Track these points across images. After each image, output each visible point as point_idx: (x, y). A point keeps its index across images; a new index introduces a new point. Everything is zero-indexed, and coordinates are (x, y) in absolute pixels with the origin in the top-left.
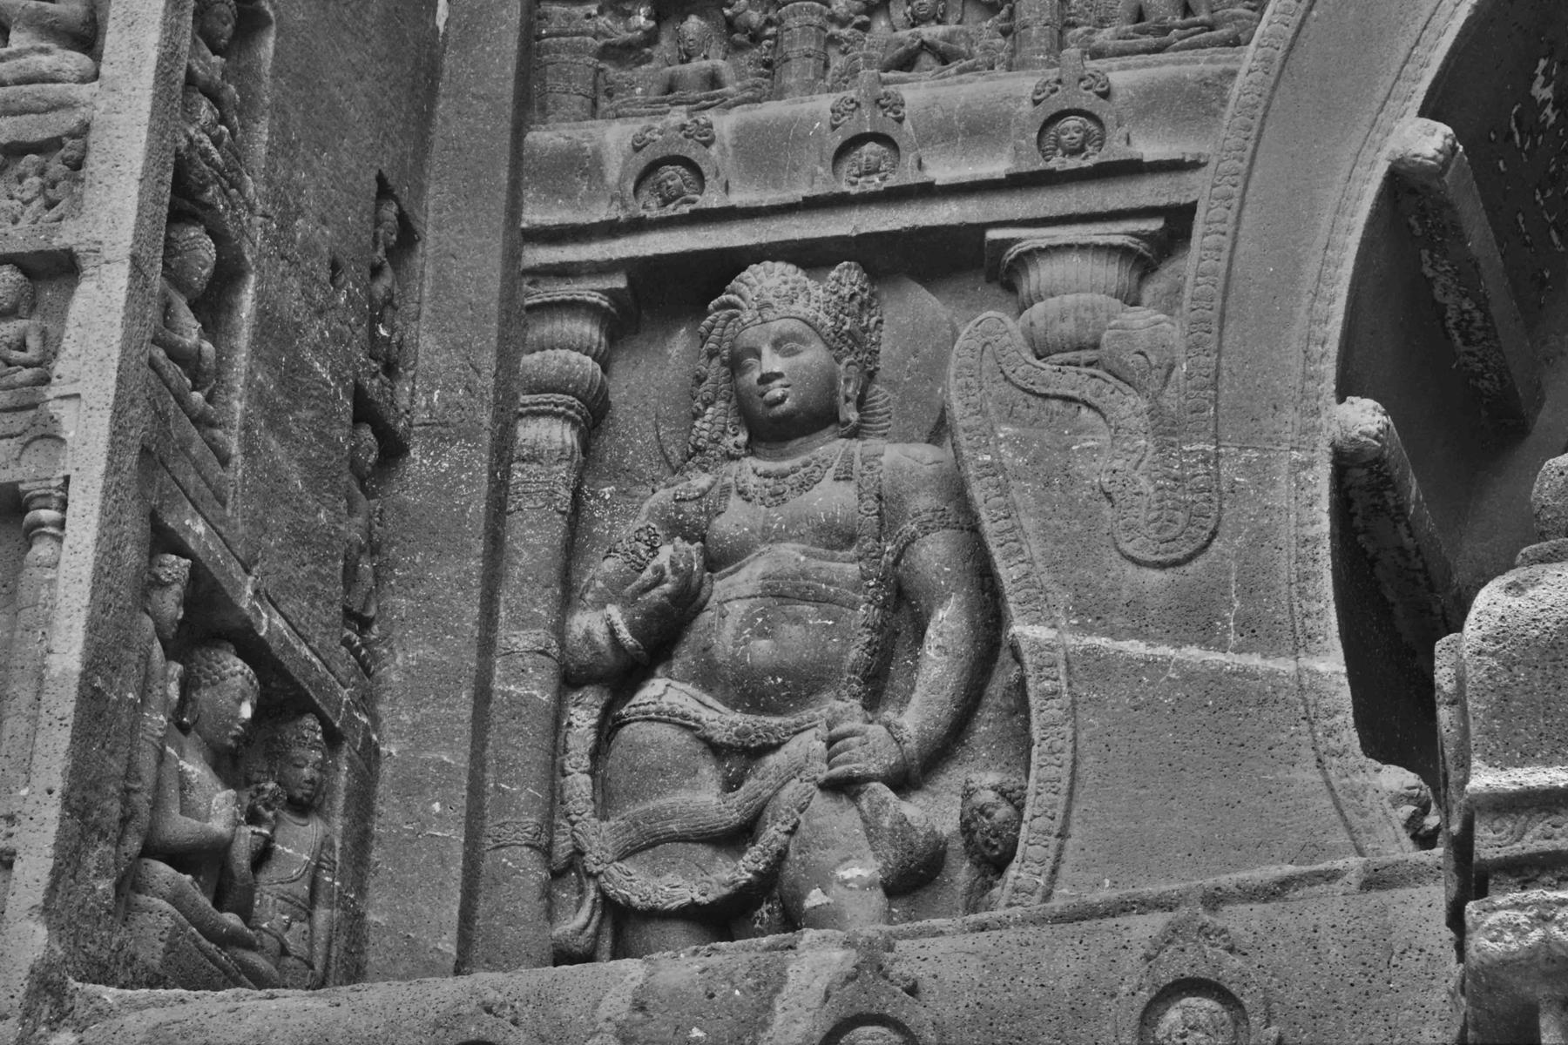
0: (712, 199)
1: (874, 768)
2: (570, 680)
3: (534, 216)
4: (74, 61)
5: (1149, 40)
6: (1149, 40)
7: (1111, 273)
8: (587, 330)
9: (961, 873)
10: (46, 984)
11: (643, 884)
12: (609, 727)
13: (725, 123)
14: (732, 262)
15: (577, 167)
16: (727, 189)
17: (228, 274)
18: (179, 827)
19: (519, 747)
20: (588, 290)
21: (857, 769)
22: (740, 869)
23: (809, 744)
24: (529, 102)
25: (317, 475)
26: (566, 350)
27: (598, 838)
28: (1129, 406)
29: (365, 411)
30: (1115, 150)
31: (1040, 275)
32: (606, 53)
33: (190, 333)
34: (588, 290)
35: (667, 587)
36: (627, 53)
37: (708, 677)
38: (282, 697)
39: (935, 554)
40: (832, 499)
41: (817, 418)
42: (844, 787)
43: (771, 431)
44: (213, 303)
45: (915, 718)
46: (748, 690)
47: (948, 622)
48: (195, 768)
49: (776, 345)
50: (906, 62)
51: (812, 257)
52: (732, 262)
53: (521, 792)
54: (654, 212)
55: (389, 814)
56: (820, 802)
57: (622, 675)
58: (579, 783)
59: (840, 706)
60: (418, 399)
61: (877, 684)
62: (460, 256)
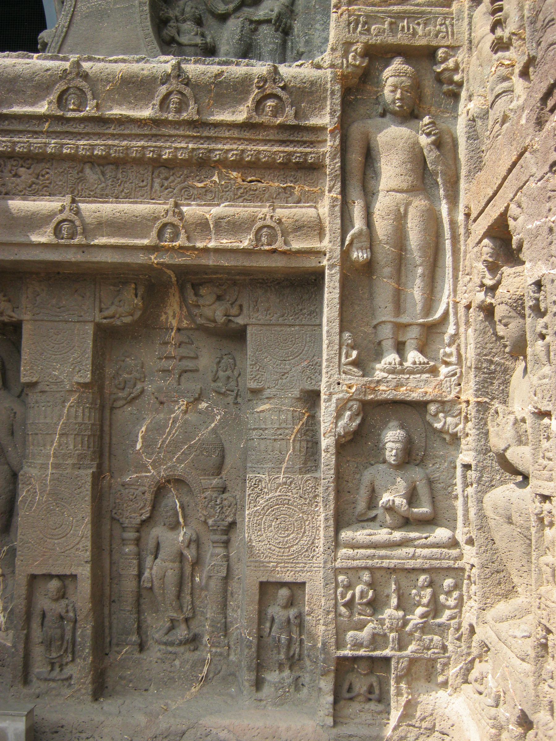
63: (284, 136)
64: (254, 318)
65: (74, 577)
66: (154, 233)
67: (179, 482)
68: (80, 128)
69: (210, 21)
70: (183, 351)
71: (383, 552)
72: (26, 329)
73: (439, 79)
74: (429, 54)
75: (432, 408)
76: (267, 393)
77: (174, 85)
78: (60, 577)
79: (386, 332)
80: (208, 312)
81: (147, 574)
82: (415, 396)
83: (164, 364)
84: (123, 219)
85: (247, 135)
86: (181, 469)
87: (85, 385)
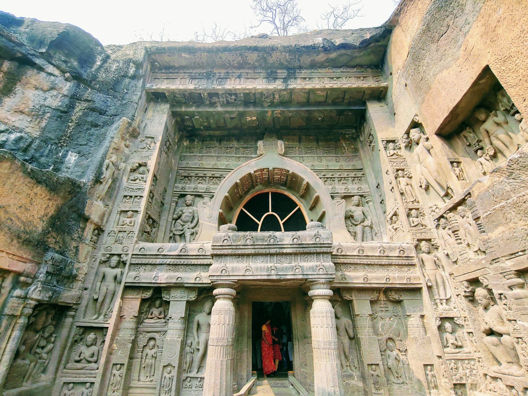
2: (173, 219)
3: (175, 190)
4: (144, 183)
7: (209, 198)
8: (177, 198)
9: (195, 234)
10: (136, 242)
11: (176, 233)
12: (175, 223)
13: (187, 185)
14: (187, 195)
15: (177, 187)
17: (153, 196)
18: (146, 230)
19: (169, 224)
22: (182, 232)
23: (187, 225)
24: (175, 182)
25: (158, 208)
27: (174, 229)
28: (208, 208)
29: (162, 202)
33: (150, 200)
37: (181, 220)
38: (154, 221)
39: (196, 215)
40: (190, 210)
41: (190, 205)
43: (188, 206)
44: (152, 198)
45: (193, 224)
46: (184, 222)
47: (196, 219)
48: (148, 226)
51: (191, 195)
52: (187, 195)
53: (169, 226)
55: (160, 228)
57: (177, 220)
58: (173, 226)
59: (189, 223)
60: (165, 202)
61: (192, 222)
62: (169, 192)
63: (406, 259)
64: (404, 297)
65: (378, 364)
66: (385, 280)
67: (390, 339)
68: (363, 258)
69: (353, 226)
70: (385, 306)
71: (455, 355)
72: (354, 301)
73: (433, 245)
74: (430, 240)
75: (456, 319)
76: (412, 316)
77: (381, 248)
78: (374, 365)
79: (438, 301)
80: (394, 297)
81: (389, 364)
82: (451, 316)
83: (381, 309)
84: (378, 277)
85: (398, 258)
86: (391, 336)
87: (370, 315)
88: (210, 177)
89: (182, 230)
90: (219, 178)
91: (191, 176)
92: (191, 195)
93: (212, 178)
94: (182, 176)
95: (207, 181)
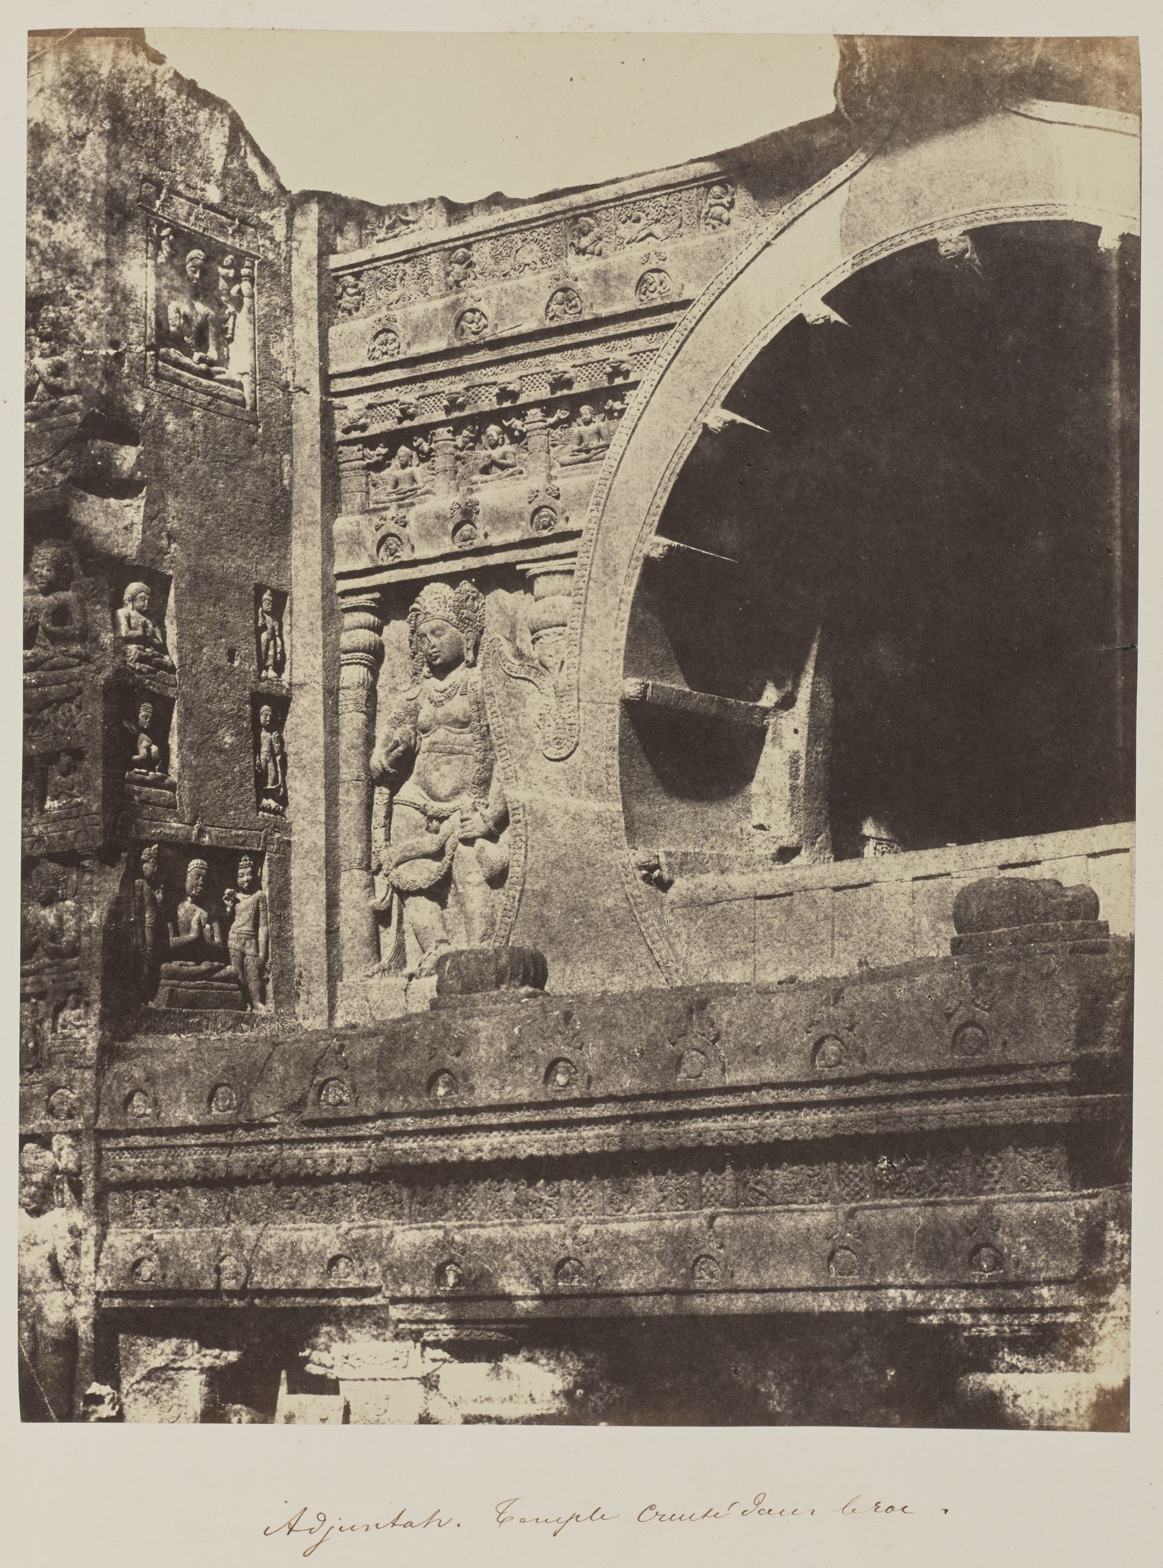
0: (405, 555)
1: (477, 834)
5: (584, 456)
6: (584, 456)
8: (370, 618)
14: (417, 586)
16: (413, 548)
20: (363, 599)
21: (472, 834)
26: (356, 632)
30: (561, 526)
31: (540, 585)
32: (369, 467)
34: (363, 599)
35: (401, 748)
36: (379, 466)
42: (468, 841)
49: (433, 632)
50: (485, 470)
51: (452, 579)
52: (417, 586)
54: (385, 559)
56: (460, 846)
58: (378, 834)
88: (547, 407)
89: (438, 855)
90: (608, 396)
91: (426, 430)
92: (452, 579)
93: (561, 414)
94: (371, 442)
95: (537, 441)
